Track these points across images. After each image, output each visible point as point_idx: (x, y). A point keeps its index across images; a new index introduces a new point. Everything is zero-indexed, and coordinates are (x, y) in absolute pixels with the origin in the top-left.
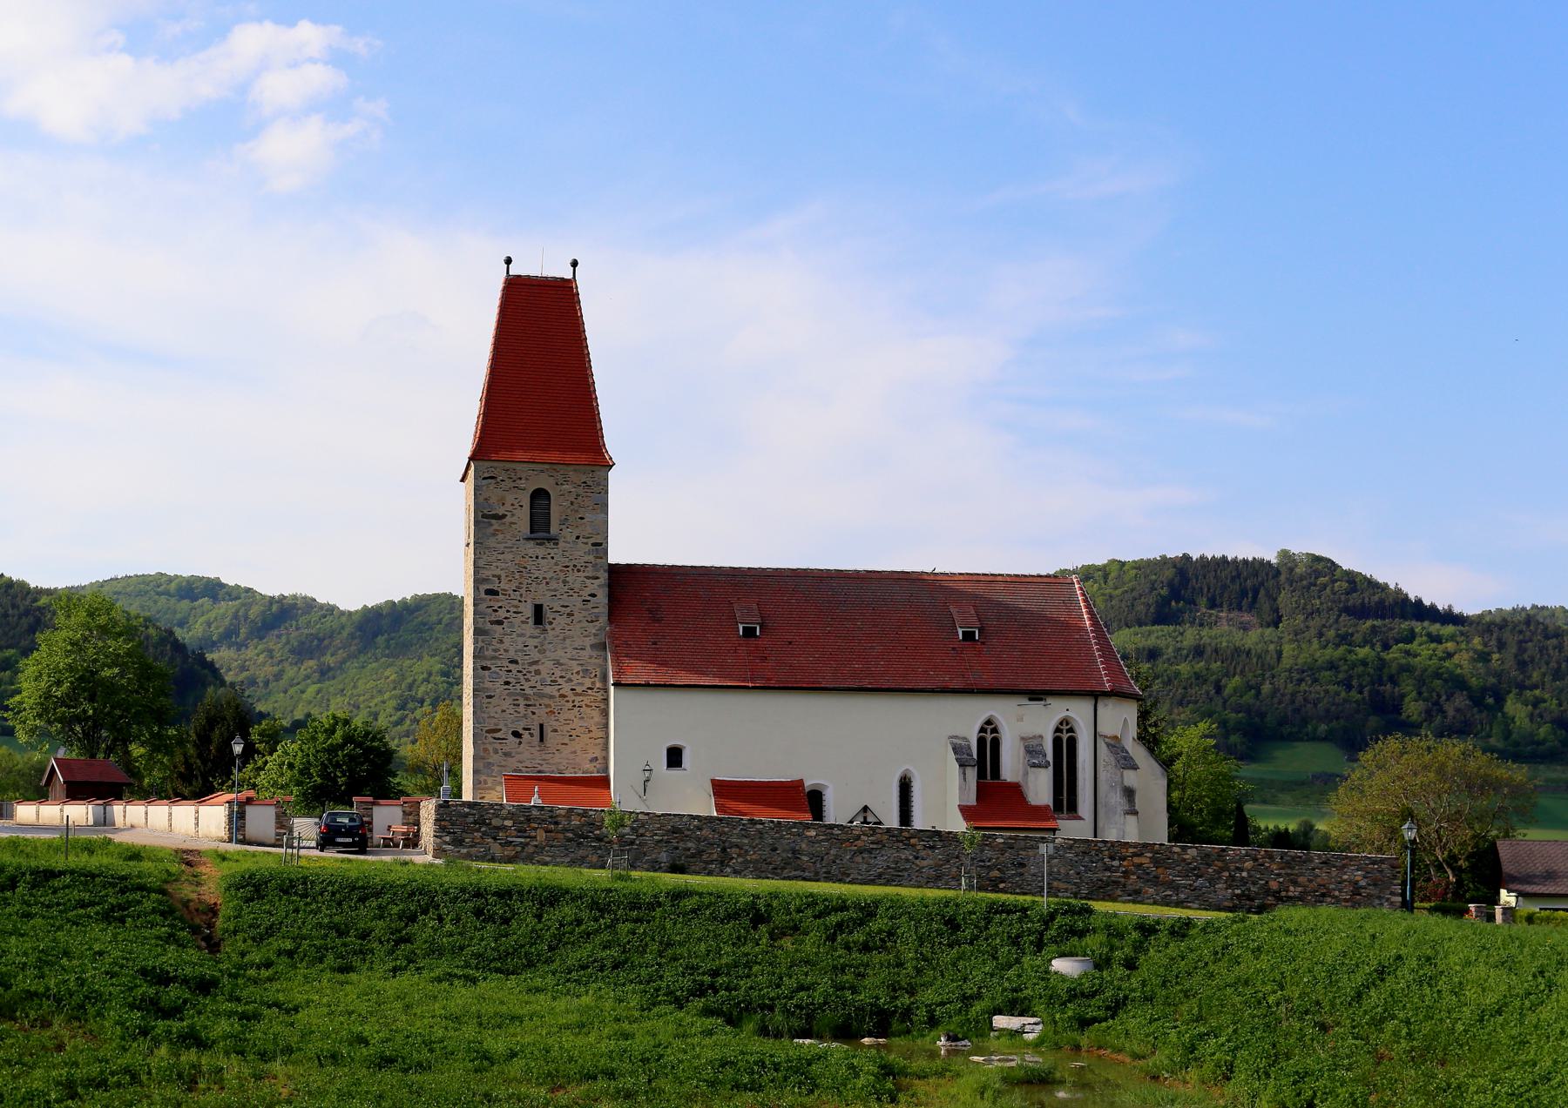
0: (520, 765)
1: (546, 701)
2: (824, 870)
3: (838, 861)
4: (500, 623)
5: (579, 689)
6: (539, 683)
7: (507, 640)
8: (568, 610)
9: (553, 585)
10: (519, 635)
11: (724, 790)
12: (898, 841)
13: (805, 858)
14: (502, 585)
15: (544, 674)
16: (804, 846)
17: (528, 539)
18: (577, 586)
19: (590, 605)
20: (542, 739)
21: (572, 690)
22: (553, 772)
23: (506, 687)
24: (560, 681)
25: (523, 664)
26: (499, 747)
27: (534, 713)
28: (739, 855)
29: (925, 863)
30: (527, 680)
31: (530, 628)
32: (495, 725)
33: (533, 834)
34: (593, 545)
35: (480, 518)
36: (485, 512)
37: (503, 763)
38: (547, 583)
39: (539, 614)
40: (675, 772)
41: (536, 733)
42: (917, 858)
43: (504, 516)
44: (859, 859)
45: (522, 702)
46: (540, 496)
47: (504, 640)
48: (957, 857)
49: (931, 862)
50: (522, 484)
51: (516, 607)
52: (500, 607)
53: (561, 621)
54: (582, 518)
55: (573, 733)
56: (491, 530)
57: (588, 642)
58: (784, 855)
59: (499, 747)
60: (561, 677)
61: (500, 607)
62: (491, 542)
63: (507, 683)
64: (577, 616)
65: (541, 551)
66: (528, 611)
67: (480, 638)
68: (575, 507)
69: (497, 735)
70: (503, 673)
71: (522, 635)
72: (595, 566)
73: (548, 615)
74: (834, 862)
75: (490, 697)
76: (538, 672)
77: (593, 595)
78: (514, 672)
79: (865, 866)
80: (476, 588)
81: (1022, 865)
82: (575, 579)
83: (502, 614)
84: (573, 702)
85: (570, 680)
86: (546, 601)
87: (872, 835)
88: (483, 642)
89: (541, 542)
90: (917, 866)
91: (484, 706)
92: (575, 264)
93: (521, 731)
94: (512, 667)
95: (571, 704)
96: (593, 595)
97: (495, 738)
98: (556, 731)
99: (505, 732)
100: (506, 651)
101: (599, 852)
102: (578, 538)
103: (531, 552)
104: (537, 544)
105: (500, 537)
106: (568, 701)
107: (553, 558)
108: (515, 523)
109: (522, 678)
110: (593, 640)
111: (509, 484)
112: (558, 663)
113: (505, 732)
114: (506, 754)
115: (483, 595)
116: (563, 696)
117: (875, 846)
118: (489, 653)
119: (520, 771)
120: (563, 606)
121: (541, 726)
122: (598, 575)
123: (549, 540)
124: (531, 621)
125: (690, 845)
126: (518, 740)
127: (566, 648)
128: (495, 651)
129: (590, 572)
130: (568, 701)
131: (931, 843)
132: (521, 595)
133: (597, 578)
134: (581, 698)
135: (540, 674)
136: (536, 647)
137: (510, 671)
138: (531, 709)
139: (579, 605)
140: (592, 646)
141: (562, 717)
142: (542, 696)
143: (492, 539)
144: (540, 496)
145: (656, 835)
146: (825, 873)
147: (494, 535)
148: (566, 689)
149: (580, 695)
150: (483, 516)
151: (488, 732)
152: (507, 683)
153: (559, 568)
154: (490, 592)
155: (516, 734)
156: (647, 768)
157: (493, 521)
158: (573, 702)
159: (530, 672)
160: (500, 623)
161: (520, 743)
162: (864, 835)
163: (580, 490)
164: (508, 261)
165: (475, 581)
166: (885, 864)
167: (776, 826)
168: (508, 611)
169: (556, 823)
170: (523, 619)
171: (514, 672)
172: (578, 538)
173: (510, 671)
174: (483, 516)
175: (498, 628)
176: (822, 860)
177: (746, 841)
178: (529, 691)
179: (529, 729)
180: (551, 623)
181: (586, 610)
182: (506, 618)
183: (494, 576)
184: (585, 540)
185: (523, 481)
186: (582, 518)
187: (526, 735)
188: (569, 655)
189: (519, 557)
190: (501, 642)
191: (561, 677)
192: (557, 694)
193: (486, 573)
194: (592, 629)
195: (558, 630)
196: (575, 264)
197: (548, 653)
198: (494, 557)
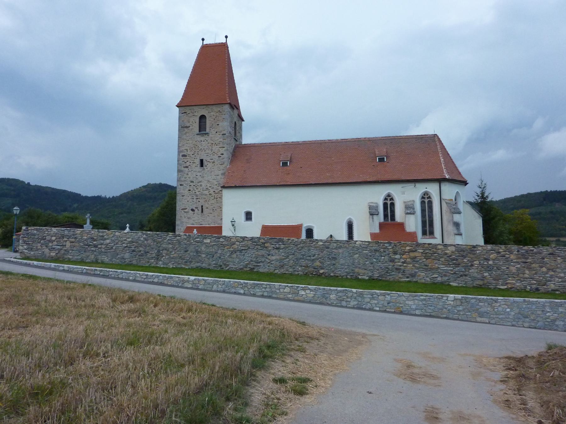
0: (194, 222)
1: (204, 196)
2: (214, 262)
3: (222, 257)
4: (187, 167)
5: (217, 191)
6: (201, 190)
7: (189, 173)
8: (213, 161)
9: (207, 151)
10: (194, 172)
11: (266, 229)
12: (257, 245)
13: (204, 256)
14: (189, 153)
15: (203, 185)
16: (203, 248)
17: (198, 134)
18: (216, 151)
19: (221, 158)
20: (202, 212)
21: (214, 192)
22: (206, 225)
23: (189, 192)
24: (210, 188)
25: (196, 182)
26: (186, 215)
27: (199, 201)
28: (167, 254)
29: (274, 258)
30: (197, 189)
31: (199, 168)
32: (185, 206)
33: (64, 244)
34: (222, 135)
35: (180, 128)
36: (182, 125)
37: (187, 222)
38: (205, 151)
39: (202, 164)
40: (249, 222)
41: (200, 209)
42: (269, 255)
43: (189, 127)
44: (234, 256)
45: (195, 197)
46: (202, 118)
47: (189, 174)
48: (293, 254)
49: (278, 257)
50: (196, 114)
51: (194, 161)
52: (187, 161)
53: (210, 165)
54: (218, 125)
55: (214, 209)
56: (184, 132)
57: (220, 172)
58: (192, 254)
59: (186, 215)
60: (210, 187)
61: (187, 161)
62: (184, 137)
63: (190, 190)
64: (216, 163)
65: (202, 138)
66: (198, 162)
67: (179, 173)
68: (216, 120)
69: (185, 211)
70: (188, 187)
71: (195, 171)
72: (223, 143)
73: (205, 163)
74: (220, 258)
75: (183, 196)
76: (201, 185)
77: (222, 154)
78: (192, 186)
79: (238, 260)
80: (179, 155)
81: (335, 259)
82: (215, 148)
83: (188, 164)
84: (214, 196)
85: (213, 188)
86: (204, 159)
87: (242, 242)
88: (181, 175)
89: (203, 135)
90: (269, 260)
91: (181, 199)
92: (226, 37)
93: (194, 209)
94: (191, 184)
95: (213, 197)
96: (222, 154)
97: (184, 212)
98: (207, 208)
99: (189, 209)
100: (189, 178)
101: (95, 253)
102: (216, 132)
103: (199, 139)
104: (201, 136)
105: (188, 134)
106: (212, 196)
107: (207, 141)
108: (193, 129)
109: (195, 188)
110: (222, 172)
111: (191, 114)
112: (209, 181)
113: (189, 209)
114: (189, 218)
115: (181, 157)
116: (210, 194)
117: (244, 248)
118: (183, 179)
119: (194, 225)
120: (211, 159)
121: (202, 206)
122: (224, 146)
123: (205, 134)
124: (199, 166)
125: (141, 249)
126: (193, 212)
127: (212, 175)
128: (185, 178)
129: (221, 145)
130: (212, 196)
131: (277, 246)
132: (195, 156)
133: (224, 147)
134: (217, 195)
135: (202, 186)
136: (200, 176)
137: (191, 186)
138: (198, 200)
139: (217, 158)
140: (222, 174)
141: (210, 203)
142: (202, 194)
143: (184, 136)
144: (202, 118)
145: (124, 243)
146: (215, 264)
147: (185, 134)
148: (212, 192)
149: (217, 193)
150: (182, 128)
151: (182, 209)
152: (190, 190)
153: (210, 144)
154: (184, 156)
155: (193, 210)
156: (233, 220)
157: (185, 129)
158: (214, 196)
159: (198, 186)
160: (187, 167)
161: (194, 213)
162: (237, 241)
163: (218, 114)
164: (203, 40)
165: (178, 152)
166: (250, 259)
167: (187, 238)
168: (190, 163)
169: (76, 238)
170: (196, 165)
171: (192, 186)
172: (216, 132)
173: (191, 186)
174: (182, 128)
175: (186, 169)
176: (213, 256)
177: (171, 246)
178: (198, 193)
179: (197, 208)
180: (206, 166)
181: (220, 160)
182: (189, 165)
183: (185, 149)
184: (219, 133)
185: (196, 113)
186: (218, 125)
187: (196, 210)
188: (213, 178)
189: (194, 142)
190: (188, 174)
191: (210, 187)
192: (208, 194)
193: (182, 149)
194: (222, 167)
195: (209, 169)
196: (226, 37)
197: (205, 178)
198: (185, 142)
